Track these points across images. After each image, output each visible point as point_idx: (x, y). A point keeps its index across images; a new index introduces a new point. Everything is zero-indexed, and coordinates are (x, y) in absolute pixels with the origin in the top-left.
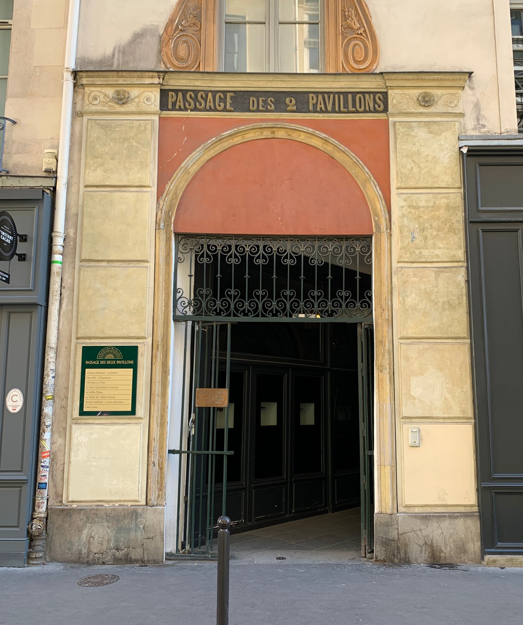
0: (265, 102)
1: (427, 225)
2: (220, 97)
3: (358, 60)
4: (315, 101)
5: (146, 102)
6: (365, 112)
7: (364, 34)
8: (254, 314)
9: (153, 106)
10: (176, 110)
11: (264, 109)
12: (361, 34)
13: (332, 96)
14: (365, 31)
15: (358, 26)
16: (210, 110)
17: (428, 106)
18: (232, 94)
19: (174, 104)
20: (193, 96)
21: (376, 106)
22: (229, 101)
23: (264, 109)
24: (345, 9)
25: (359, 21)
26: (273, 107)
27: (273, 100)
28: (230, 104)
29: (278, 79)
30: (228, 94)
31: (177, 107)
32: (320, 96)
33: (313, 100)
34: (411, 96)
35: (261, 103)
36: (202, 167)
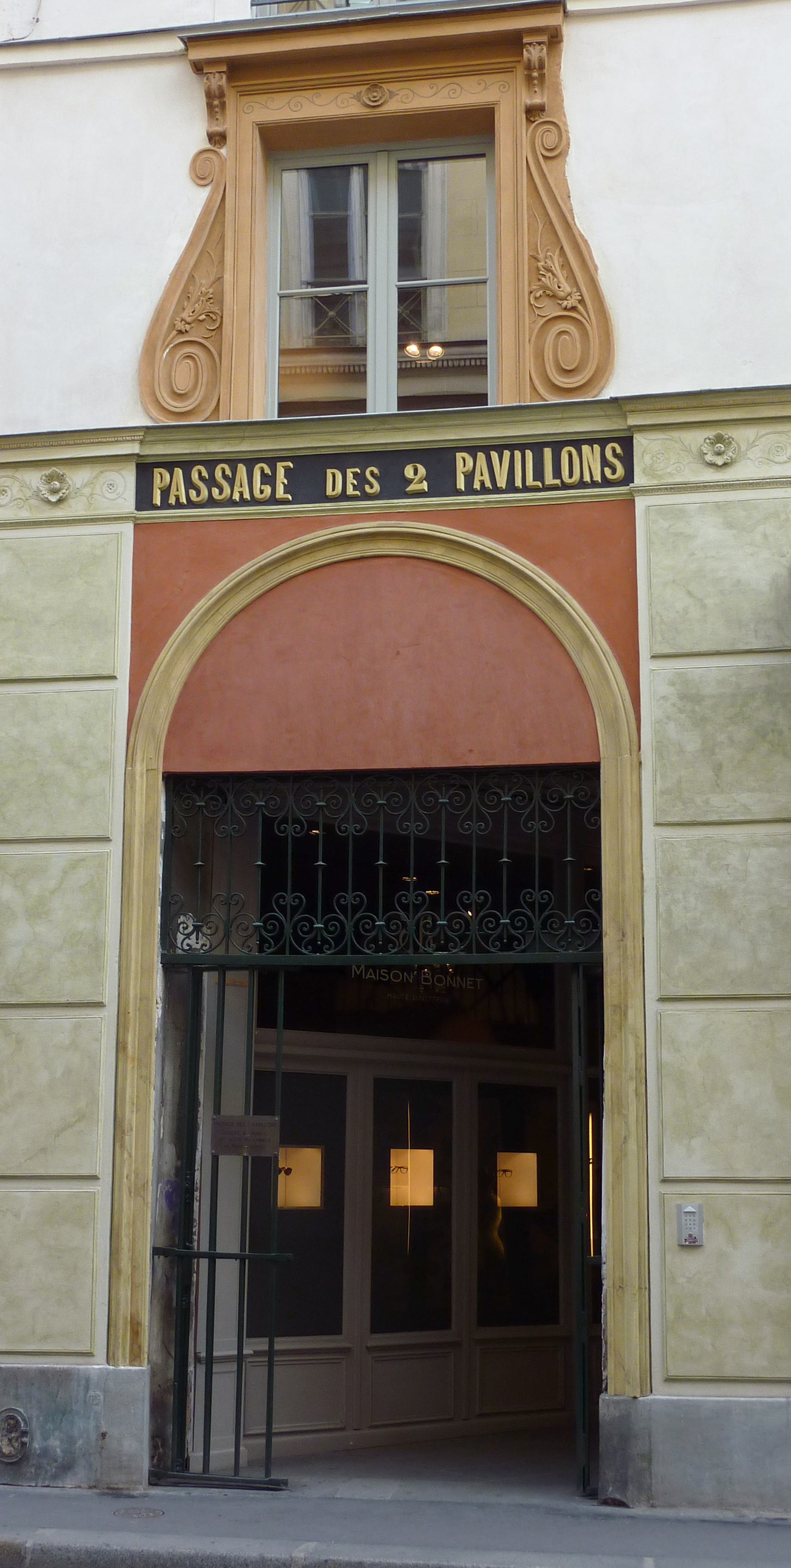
1: (721, 738)
3: (567, 368)
6: (582, 484)
7: (580, 307)
9: (120, 501)
10: (170, 507)
11: (358, 493)
12: (574, 309)
14: (582, 301)
16: (243, 502)
17: (725, 464)
19: (166, 493)
20: (205, 474)
23: (358, 493)
24: (538, 253)
25: (571, 277)
26: (377, 487)
27: (376, 471)
28: (285, 485)
29: (386, 426)
32: (481, 456)
34: (686, 444)
36: (224, 628)
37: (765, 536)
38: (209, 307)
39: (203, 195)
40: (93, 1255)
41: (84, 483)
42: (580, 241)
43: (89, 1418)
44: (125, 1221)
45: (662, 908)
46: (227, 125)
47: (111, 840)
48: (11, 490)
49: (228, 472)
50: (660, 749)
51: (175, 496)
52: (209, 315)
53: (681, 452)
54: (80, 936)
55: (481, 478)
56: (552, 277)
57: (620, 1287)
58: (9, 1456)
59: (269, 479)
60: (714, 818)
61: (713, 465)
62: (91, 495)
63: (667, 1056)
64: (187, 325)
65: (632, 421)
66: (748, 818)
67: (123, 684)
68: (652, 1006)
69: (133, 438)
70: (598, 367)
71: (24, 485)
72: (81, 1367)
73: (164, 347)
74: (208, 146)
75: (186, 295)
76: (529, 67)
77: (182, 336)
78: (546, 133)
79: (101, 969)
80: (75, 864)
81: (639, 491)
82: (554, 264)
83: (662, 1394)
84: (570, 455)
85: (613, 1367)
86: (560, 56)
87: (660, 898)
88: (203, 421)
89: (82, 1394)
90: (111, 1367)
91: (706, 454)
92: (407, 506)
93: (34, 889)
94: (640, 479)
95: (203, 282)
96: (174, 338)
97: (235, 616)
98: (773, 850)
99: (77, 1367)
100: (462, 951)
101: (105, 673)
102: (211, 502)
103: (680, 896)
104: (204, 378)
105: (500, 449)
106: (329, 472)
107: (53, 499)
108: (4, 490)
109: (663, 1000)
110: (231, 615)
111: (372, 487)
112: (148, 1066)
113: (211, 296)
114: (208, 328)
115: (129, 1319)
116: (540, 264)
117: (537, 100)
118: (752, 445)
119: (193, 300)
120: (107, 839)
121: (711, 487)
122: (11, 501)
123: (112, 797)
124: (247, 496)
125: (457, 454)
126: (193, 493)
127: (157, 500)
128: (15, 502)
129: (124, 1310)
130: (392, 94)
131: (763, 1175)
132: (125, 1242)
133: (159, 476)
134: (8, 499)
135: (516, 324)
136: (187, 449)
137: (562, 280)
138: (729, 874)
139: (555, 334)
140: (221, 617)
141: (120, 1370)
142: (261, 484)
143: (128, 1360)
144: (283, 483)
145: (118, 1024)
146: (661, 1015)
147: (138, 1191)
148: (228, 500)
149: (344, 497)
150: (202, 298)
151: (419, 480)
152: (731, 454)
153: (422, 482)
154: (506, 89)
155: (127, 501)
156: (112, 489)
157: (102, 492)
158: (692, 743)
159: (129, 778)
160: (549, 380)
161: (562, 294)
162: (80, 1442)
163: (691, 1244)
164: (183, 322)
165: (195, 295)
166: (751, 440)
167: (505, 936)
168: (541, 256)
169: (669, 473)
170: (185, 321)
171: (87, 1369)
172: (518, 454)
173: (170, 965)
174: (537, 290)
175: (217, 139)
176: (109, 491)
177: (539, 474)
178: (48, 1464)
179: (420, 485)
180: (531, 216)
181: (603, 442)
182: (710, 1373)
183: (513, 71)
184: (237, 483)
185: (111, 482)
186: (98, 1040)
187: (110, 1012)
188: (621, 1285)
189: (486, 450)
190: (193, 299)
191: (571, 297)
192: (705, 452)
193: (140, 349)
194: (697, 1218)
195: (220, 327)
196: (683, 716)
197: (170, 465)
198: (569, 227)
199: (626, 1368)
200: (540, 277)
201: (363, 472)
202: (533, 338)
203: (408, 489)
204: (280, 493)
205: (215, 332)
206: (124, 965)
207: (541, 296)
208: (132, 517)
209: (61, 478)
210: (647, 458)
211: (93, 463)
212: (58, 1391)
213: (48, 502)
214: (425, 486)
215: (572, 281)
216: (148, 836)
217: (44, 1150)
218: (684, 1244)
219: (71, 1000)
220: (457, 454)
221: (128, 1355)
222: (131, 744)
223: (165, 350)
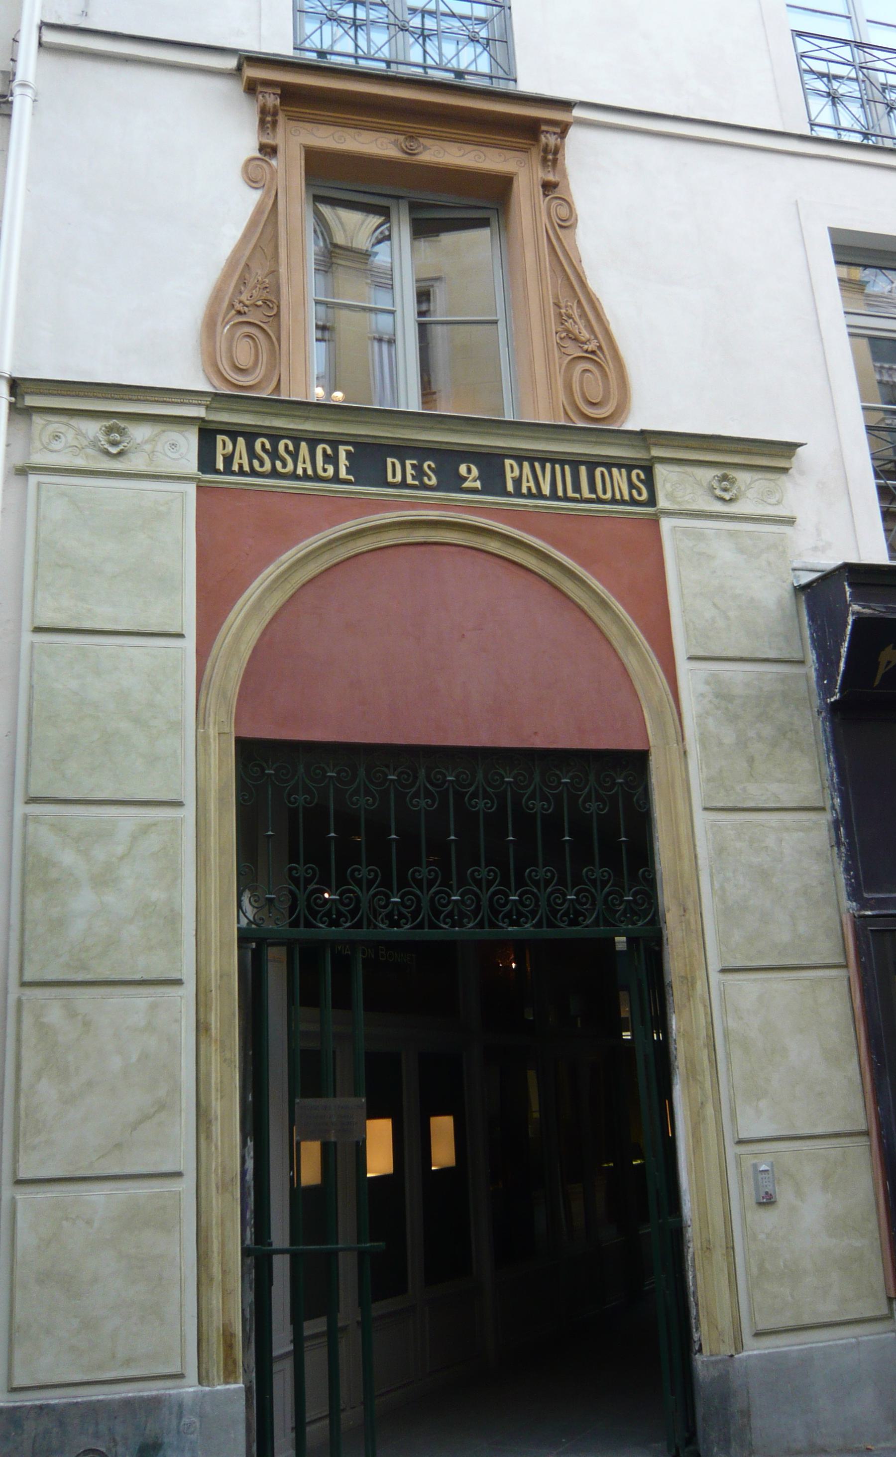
0: (418, 468)
1: (751, 733)
2: (324, 451)
4: (517, 473)
5: (170, 454)
6: (613, 501)
7: (598, 352)
8: (413, 922)
10: (233, 473)
11: (417, 483)
12: (593, 352)
13: (548, 465)
15: (588, 336)
16: (306, 477)
17: (731, 500)
19: (228, 460)
20: (268, 446)
21: (634, 492)
23: (417, 483)
26: (434, 481)
27: (433, 465)
28: (347, 467)
29: (443, 426)
31: (235, 468)
32: (526, 465)
33: (512, 471)
35: (409, 471)
36: (292, 596)
37: (769, 564)
38: (265, 295)
40: (181, 1262)
41: (146, 438)
43: (183, 1451)
45: (717, 886)
46: (278, 139)
47: (184, 805)
48: (65, 436)
49: (291, 448)
50: (704, 740)
52: (266, 303)
53: (694, 485)
54: (153, 907)
55: (528, 485)
56: (573, 323)
57: (707, 1248)
61: (722, 499)
62: (153, 452)
63: (732, 1024)
64: (245, 308)
65: (656, 452)
66: (778, 805)
67: (190, 643)
68: (715, 977)
69: (200, 402)
70: (618, 405)
71: (79, 433)
72: (172, 1392)
73: (224, 323)
75: (243, 281)
76: (546, 150)
77: (240, 316)
78: (559, 207)
79: (179, 943)
80: (145, 829)
82: (574, 313)
83: (754, 1349)
85: (706, 1327)
87: (714, 877)
88: (268, 395)
89: (174, 1422)
90: (207, 1389)
91: (715, 489)
92: (464, 500)
93: (100, 853)
94: (663, 503)
95: (259, 272)
96: (233, 316)
97: (304, 585)
98: (801, 834)
99: (167, 1392)
101: (172, 630)
102: (274, 474)
103: (729, 874)
104: (264, 358)
106: (389, 460)
107: (114, 450)
108: (57, 436)
109: (724, 971)
110: (300, 585)
113: (268, 286)
114: (266, 314)
115: (221, 1332)
116: (563, 311)
117: (551, 177)
118: (749, 487)
120: (179, 804)
122: (66, 447)
123: (184, 759)
124: (310, 472)
126: (256, 463)
128: (70, 449)
129: (217, 1321)
131: (819, 1130)
132: (216, 1246)
133: (221, 443)
135: (545, 356)
136: (252, 420)
137: (582, 327)
138: (768, 855)
139: (580, 371)
140: (290, 586)
141: (217, 1390)
142: (324, 464)
143: (222, 1378)
146: (724, 985)
148: (291, 475)
149: (404, 484)
150: (258, 286)
151: (473, 478)
152: (735, 492)
153: (475, 481)
154: (523, 165)
156: (175, 449)
157: (164, 450)
158: (729, 737)
159: (201, 741)
161: (583, 339)
163: (767, 1201)
164: (241, 304)
165: (252, 282)
166: (748, 482)
168: (563, 305)
169: (687, 501)
170: (243, 303)
171: (180, 1393)
172: (557, 467)
174: (562, 332)
175: (268, 150)
176: (172, 450)
179: (474, 483)
180: (552, 270)
182: (792, 1323)
183: (528, 152)
184: (300, 459)
185: (174, 442)
186: (178, 1021)
187: (189, 989)
188: (708, 1247)
190: (250, 285)
191: (590, 343)
192: (715, 487)
193: (199, 322)
194: (770, 1175)
195: (278, 315)
196: (719, 712)
197: (233, 434)
199: (719, 1327)
201: (421, 466)
202: (562, 371)
203: (463, 486)
204: (343, 474)
205: (272, 318)
206: (203, 938)
207: (564, 337)
208: (197, 478)
210: (668, 486)
213: (107, 453)
214: (478, 484)
217: (118, 1146)
218: (762, 1201)
219: (146, 977)
222: (202, 705)
223: (225, 327)
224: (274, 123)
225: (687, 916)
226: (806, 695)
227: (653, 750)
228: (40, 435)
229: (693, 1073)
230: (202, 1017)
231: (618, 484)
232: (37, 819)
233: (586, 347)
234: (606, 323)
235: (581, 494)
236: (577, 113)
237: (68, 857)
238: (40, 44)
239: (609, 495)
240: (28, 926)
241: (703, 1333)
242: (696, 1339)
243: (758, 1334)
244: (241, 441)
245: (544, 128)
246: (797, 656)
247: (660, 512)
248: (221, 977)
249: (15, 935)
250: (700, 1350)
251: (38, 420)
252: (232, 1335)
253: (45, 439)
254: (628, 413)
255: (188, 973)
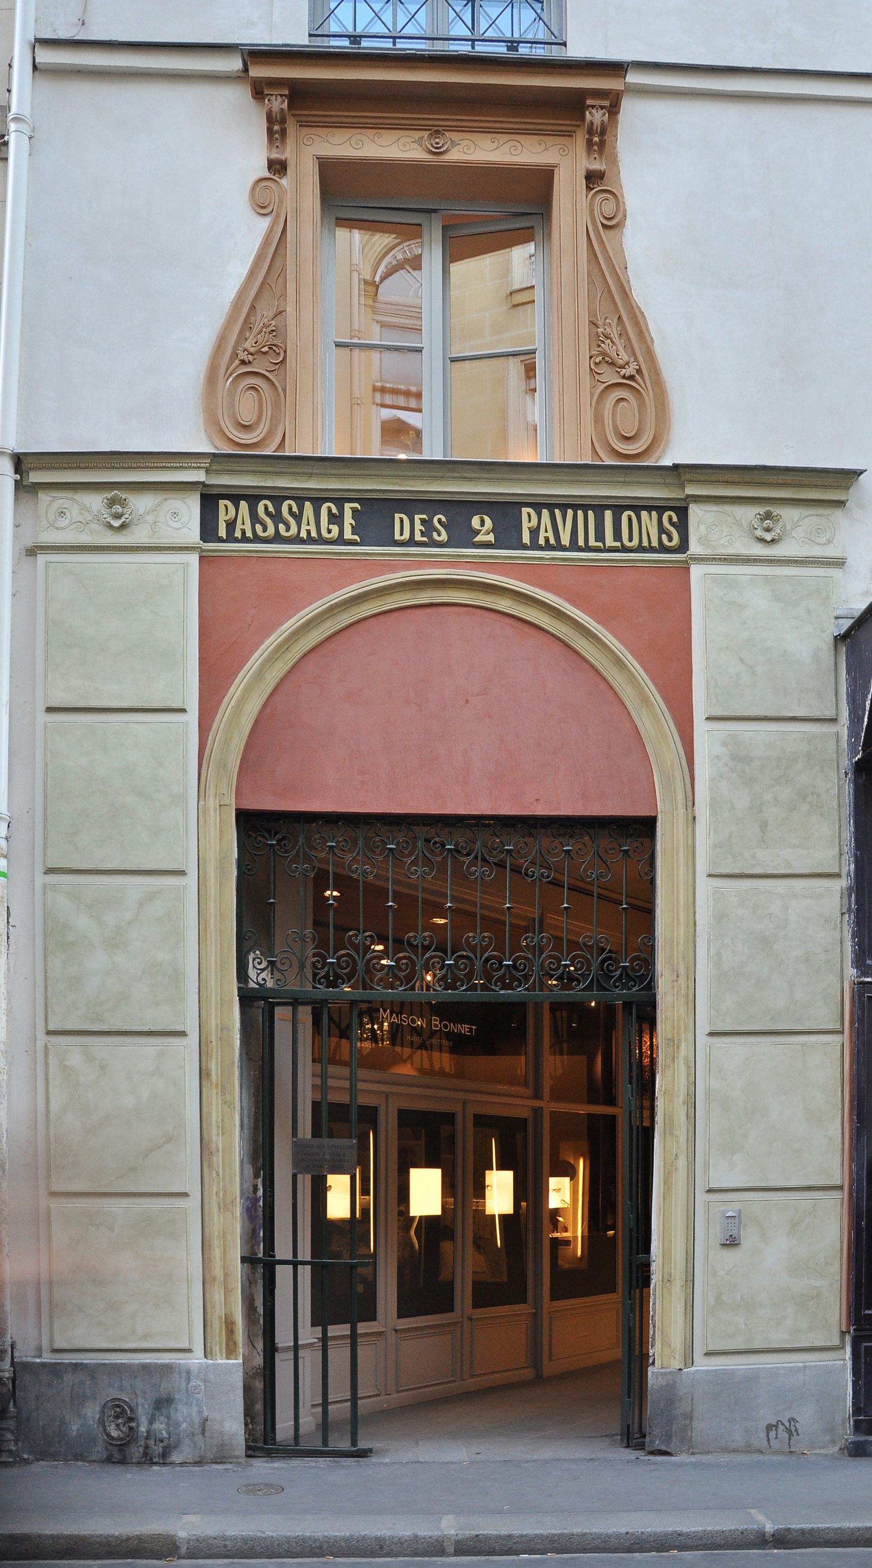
6: (640, 549)
7: (637, 376)
9: (185, 530)
10: (236, 540)
11: (425, 539)
13: (570, 512)
14: (639, 371)
16: (310, 540)
17: (773, 541)
18: (356, 505)
19: (231, 525)
20: (271, 509)
21: (664, 537)
22: (348, 519)
23: (425, 539)
26: (444, 537)
27: (444, 519)
28: (353, 527)
30: (348, 506)
32: (545, 512)
33: (530, 521)
35: (418, 526)
36: (294, 667)
37: (809, 611)
39: (264, 224)
41: (148, 509)
42: (638, 313)
43: (191, 1405)
44: (216, 1234)
46: (287, 153)
48: (71, 513)
49: (295, 509)
51: (241, 529)
52: (272, 348)
53: (733, 525)
55: (546, 535)
58: (119, 1439)
59: (336, 519)
60: (759, 871)
61: (761, 540)
62: (155, 522)
65: (690, 490)
67: (192, 717)
71: (84, 508)
72: (181, 1362)
74: (267, 174)
75: (247, 325)
77: (244, 366)
81: (695, 559)
84: (630, 520)
86: (616, 127)
89: (184, 1384)
90: (210, 1362)
91: (756, 529)
92: (475, 556)
94: (695, 548)
96: (237, 367)
99: (178, 1361)
100: (526, 989)
101: (175, 705)
102: (278, 538)
104: (268, 412)
105: (564, 507)
106: (397, 516)
107: (116, 523)
108: (62, 512)
111: (439, 535)
112: (232, 1093)
113: (274, 328)
117: (596, 166)
118: (796, 525)
119: (255, 330)
120: (182, 873)
121: (761, 561)
125: (523, 509)
126: (258, 528)
127: (222, 532)
128: (76, 525)
130: (454, 144)
134: (67, 522)
141: (219, 1364)
143: (224, 1355)
144: (351, 524)
145: (200, 1053)
147: (225, 1207)
149: (411, 542)
150: (264, 329)
152: (778, 531)
153: (489, 534)
155: (192, 532)
160: (609, 445)
161: (621, 362)
162: (184, 1425)
164: (246, 353)
166: (796, 519)
167: (565, 977)
172: (580, 513)
173: (247, 998)
175: (277, 167)
177: (600, 535)
178: (155, 1445)
181: (661, 510)
184: (304, 521)
185: (174, 511)
189: (551, 507)
192: (756, 526)
195: (284, 361)
196: (734, 775)
197: (235, 499)
198: (626, 295)
200: (600, 343)
203: (475, 540)
204: (348, 535)
208: (198, 547)
209: (123, 503)
210: (702, 528)
211: (156, 489)
212: (161, 1383)
213: (111, 527)
214: (491, 538)
215: (630, 350)
216: (222, 871)
217: (133, 1169)
220: (523, 509)
221: (224, 1351)
224: (283, 133)
225: (680, 981)
226: (834, 756)
227: (659, 817)
228: (46, 512)
229: (669, 1128)
230: (204, 1064)
231: (647, 529)
232: (54, 887)
233: (623, 372)
234: (649, 342)
235: (604, 544)
236: (632, 78)
237: (83, 922)
238: (35, 67)
239: (635, 542)
240: (50, 982)
241: (656, 1350)
242: (650, 1354)
243: (708, 1354)
244: (243, 504)
245: (589, 102)
246: (829, 713)
247: (690, 558)
248: (222, 1030)
249: (40, 990)
250: (653, 1363)
251: (44, 497)
252: (233, 1323)
253: (51, 517)
254: (667, 445)
255: (191, 1026)
